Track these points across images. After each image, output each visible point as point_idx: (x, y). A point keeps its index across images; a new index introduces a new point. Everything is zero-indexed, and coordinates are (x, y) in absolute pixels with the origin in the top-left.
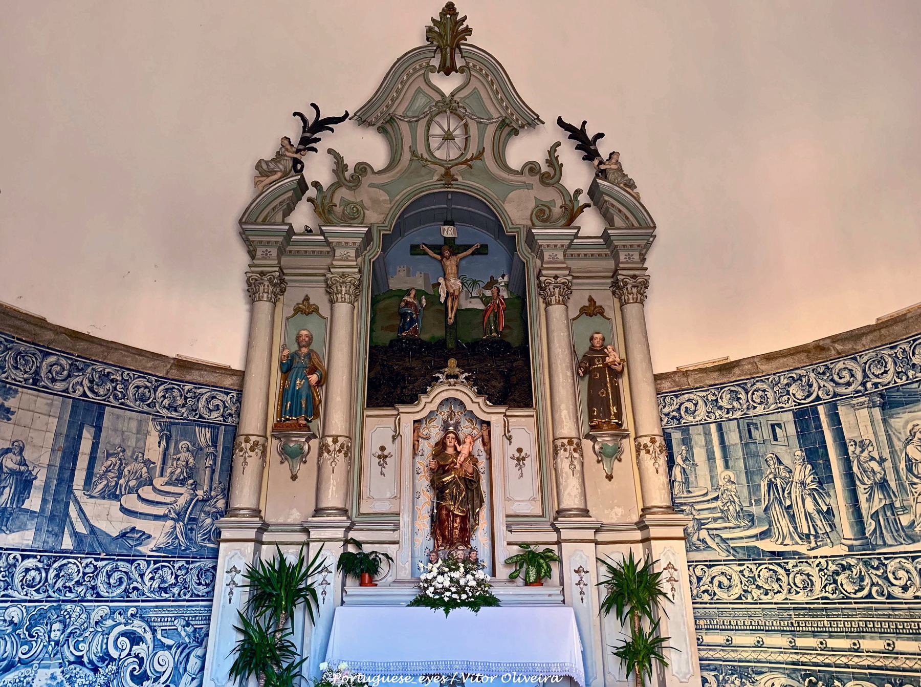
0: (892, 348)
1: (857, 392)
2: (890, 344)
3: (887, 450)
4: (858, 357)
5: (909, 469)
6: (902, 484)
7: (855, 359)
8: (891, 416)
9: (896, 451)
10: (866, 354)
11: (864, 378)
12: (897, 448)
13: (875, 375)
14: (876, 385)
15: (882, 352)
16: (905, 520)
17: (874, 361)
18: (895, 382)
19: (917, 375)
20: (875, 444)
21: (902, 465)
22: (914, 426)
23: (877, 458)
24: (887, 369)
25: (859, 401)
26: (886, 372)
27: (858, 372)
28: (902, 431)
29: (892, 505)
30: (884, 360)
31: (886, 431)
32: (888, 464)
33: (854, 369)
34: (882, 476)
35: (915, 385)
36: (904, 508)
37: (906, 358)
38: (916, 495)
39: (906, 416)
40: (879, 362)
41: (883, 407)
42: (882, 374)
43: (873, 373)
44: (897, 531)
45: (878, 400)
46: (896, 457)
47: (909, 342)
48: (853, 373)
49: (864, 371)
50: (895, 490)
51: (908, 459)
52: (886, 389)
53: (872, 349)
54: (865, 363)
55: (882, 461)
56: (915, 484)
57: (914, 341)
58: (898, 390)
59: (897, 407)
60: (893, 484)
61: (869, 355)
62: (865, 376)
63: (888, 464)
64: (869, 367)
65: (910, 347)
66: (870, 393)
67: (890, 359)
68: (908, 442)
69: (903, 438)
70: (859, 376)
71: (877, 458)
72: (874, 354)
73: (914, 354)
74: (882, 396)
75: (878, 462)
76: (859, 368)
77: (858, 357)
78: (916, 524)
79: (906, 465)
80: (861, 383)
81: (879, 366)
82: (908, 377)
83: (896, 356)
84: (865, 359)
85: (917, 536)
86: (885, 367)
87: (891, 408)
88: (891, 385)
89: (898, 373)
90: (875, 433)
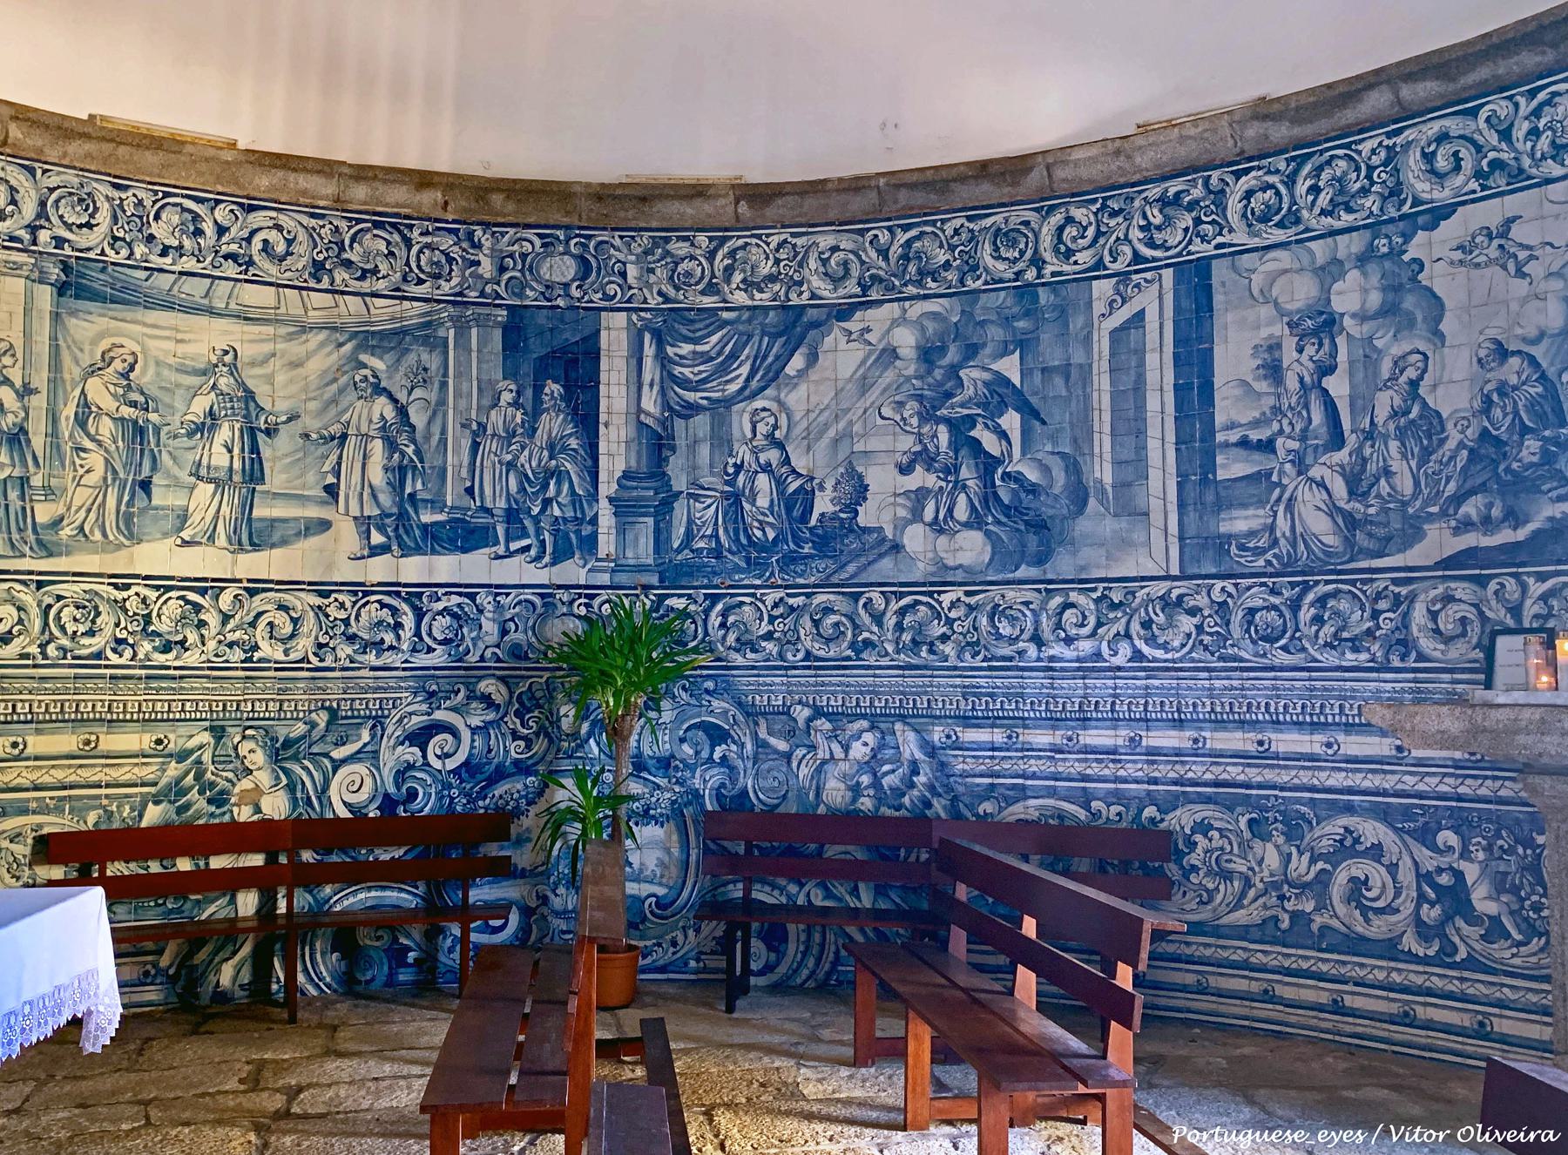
0: (116, 186)
1: (12, 239)
2: (115, 177)
3: (45, 375)
4: (39, 172)
5: (81, 422)
6: (58, 447)
7: (32, 171)
8: (74, 313)
9: (63, 381)
10: (59, 173)
11: (38, 216)
12: (67, 376)
13: (65, 223)
14: (60, 242)
15: (95, 185)
16: (44, 513)
17: (71, 194)
18: (103, 253)
19: (152, 257)
20: (19, 355)
21: (69, 411)
22: (114, 346)
23: (18, 383)
24: (93, 222)
25: (13, 258)
26: (89, 225)
27: (27, 199)
28: (87, 348)
29: (24, 482)
30: (94, 202)
31: (54, 338)
32: (39, 402)
33: (22, 190)
34: (18, 420)
35: (143, 274)
36: (49, 492)
37: (141, 218)
38: (81, 471)
39: (103, 323)
40: (81, 200)
41: (61, 289)
42: (80, 226)
43: (61, 217)
44: (20, 530)
45: (55, 272)
46: (60, 392)
47: (156, 193)
48: (18, 197)
49: (43, 204)
50: (40, 454)
51: (84, 403)
52: (78, 258)
53: (74, 168)
54: (52, 190)
55: (26, 391)
56: (84, 450)
57: (166, 195)
58: (103, 270)
59: (90, 299)
60: (38, 442)
61: (63, 177)
62: (42, 213)
63: (39, 402)
64: (57, 201)
65: (154, 202)
66: (41, 253)
67: (106, 205)
68: (93, 371)
69: (86, 361)
70: (29, 210)
71: (18, 383)
72: (76, 180)
73: (157, 217)
74: (66, 268)
75: (17, 392)
76: (33, 193)
77: (39, 172)
78: (65, 522)
79: (76, 414)
80: (28, 226)
81: (78, 208)
82: (132, 253)
83: (121, 206)
84: (53, 181)
85: (59, 545)
86: (92, 216)
87: (77, 297)
88: (91, 255)
89: (116, 239)
90: (27, 335)
